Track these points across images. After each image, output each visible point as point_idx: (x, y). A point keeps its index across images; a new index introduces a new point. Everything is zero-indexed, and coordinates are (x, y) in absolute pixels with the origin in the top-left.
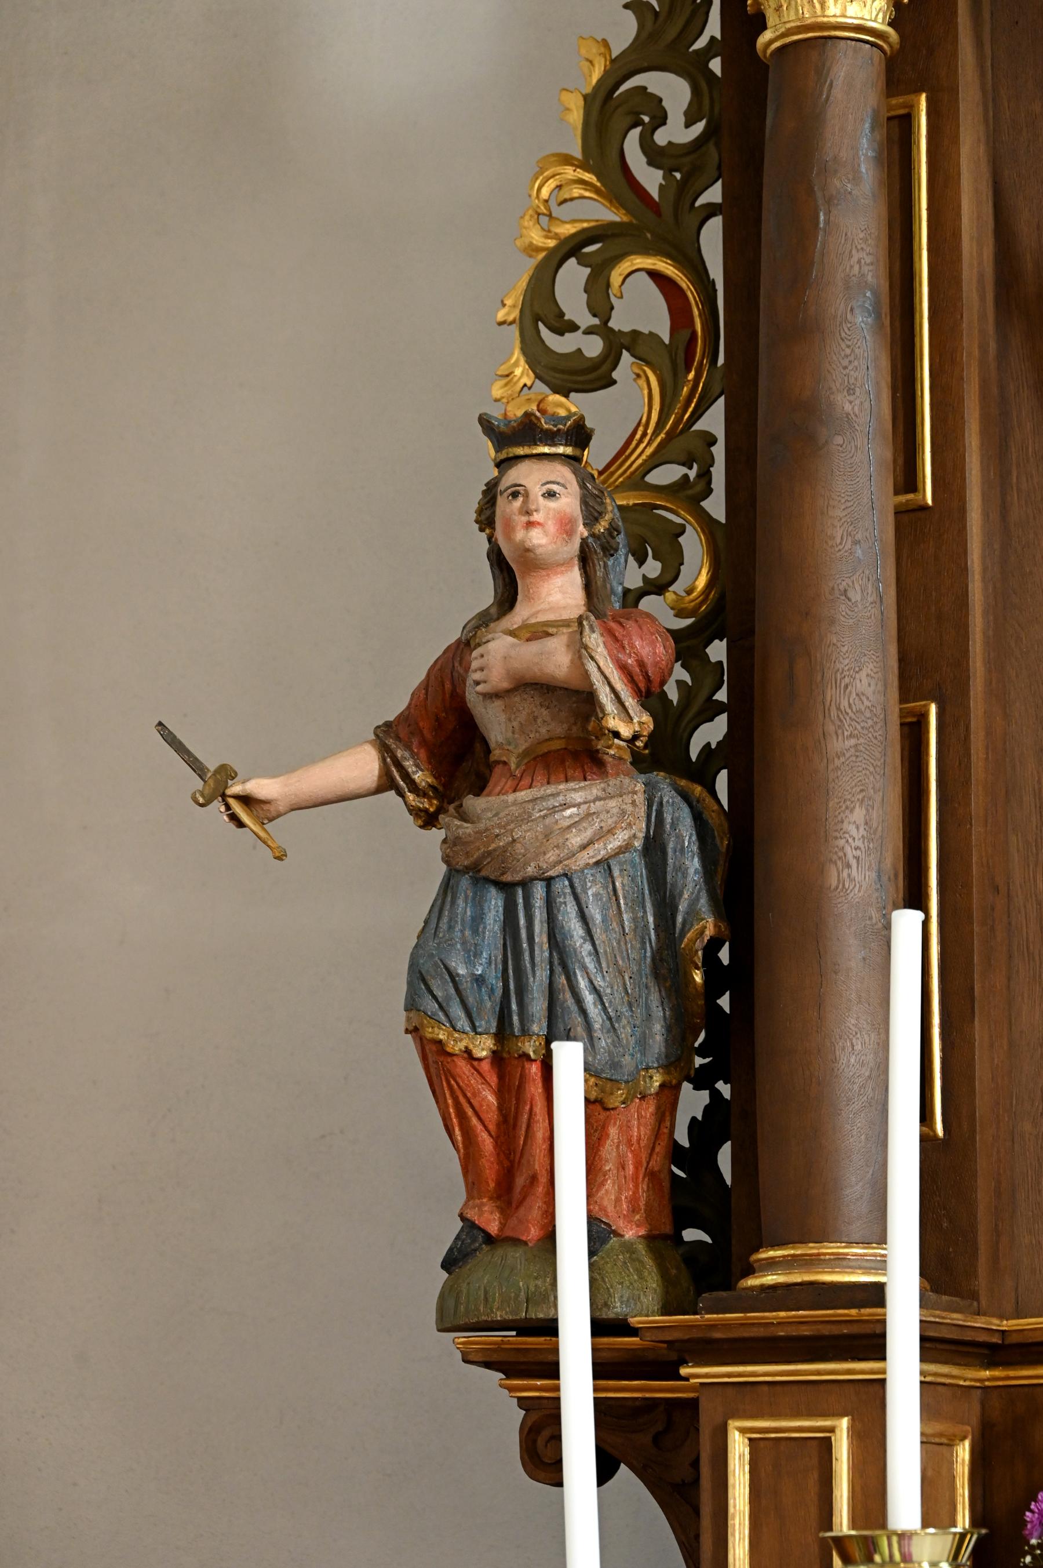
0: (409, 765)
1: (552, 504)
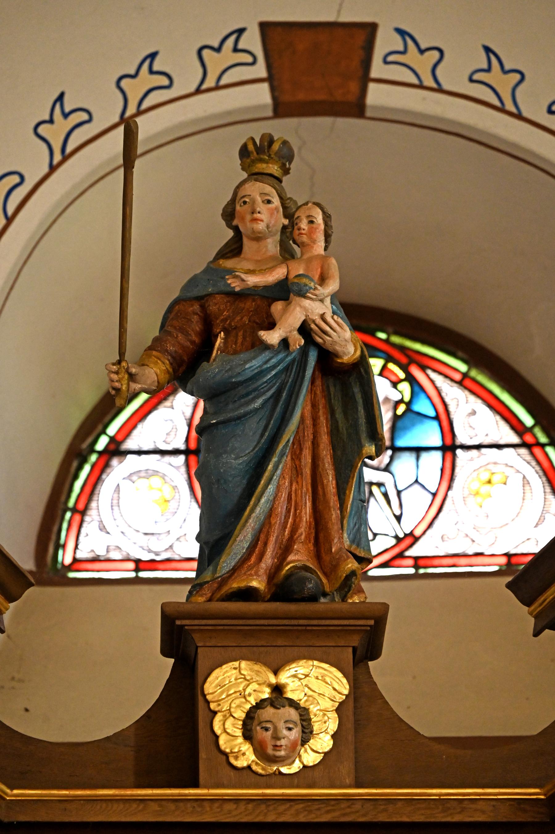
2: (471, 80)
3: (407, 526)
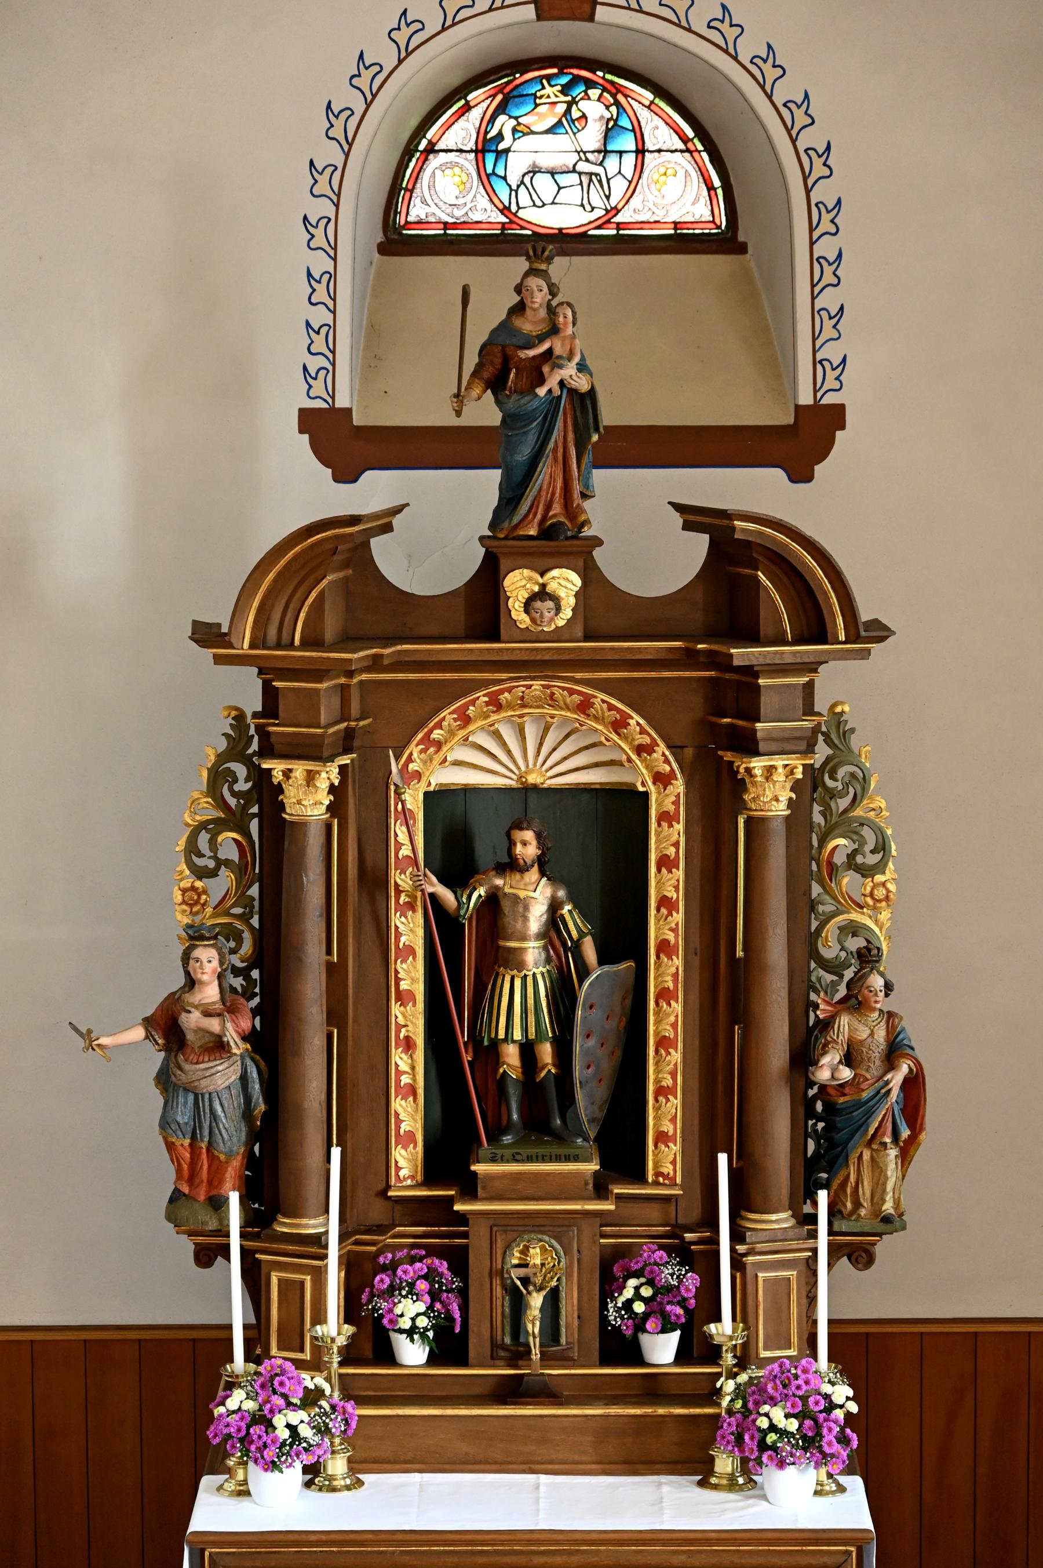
0: (156, 1037)
1: (210, 965)
3: (613, 202)
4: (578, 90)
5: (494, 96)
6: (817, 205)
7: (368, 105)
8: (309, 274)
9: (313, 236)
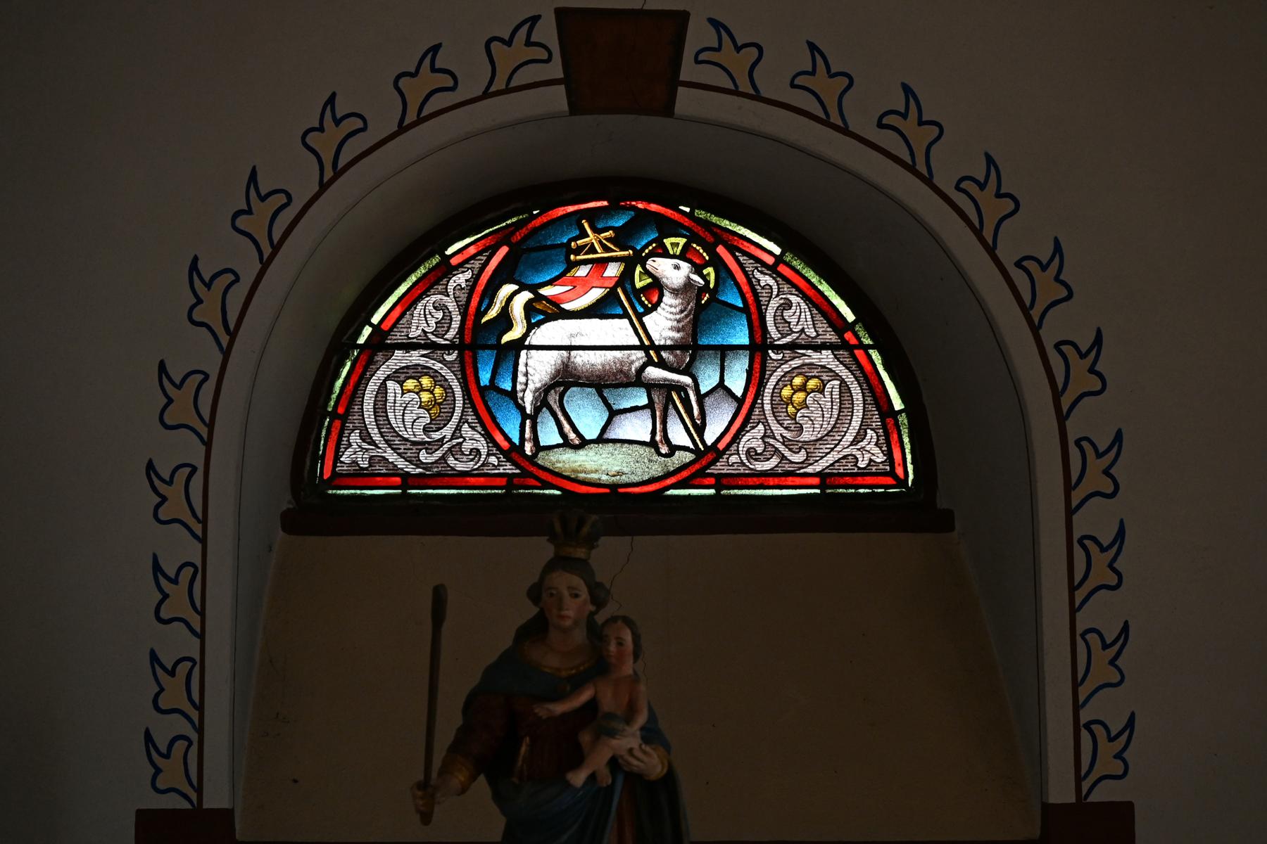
2: (793, 86)
4: (645, 240)
5: (493, 250)
6: (1078, 443)
7: (265, 265)
8: (157, 568)
9: (164, 499)
